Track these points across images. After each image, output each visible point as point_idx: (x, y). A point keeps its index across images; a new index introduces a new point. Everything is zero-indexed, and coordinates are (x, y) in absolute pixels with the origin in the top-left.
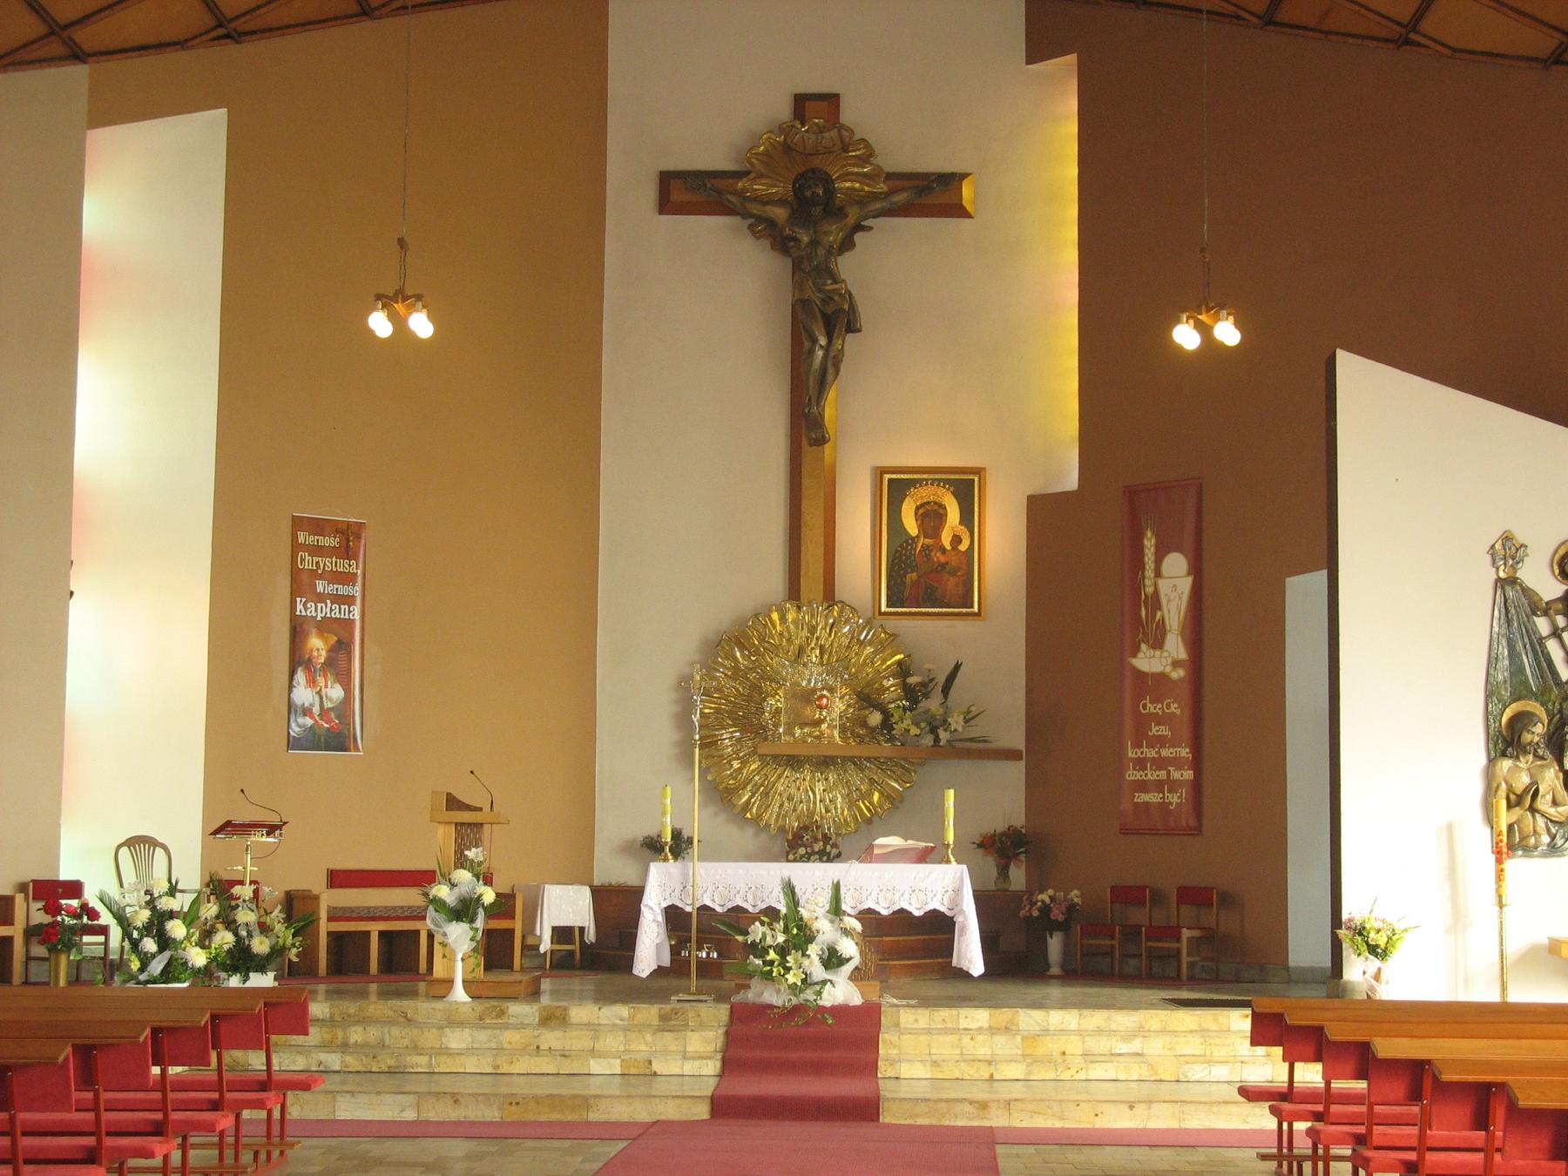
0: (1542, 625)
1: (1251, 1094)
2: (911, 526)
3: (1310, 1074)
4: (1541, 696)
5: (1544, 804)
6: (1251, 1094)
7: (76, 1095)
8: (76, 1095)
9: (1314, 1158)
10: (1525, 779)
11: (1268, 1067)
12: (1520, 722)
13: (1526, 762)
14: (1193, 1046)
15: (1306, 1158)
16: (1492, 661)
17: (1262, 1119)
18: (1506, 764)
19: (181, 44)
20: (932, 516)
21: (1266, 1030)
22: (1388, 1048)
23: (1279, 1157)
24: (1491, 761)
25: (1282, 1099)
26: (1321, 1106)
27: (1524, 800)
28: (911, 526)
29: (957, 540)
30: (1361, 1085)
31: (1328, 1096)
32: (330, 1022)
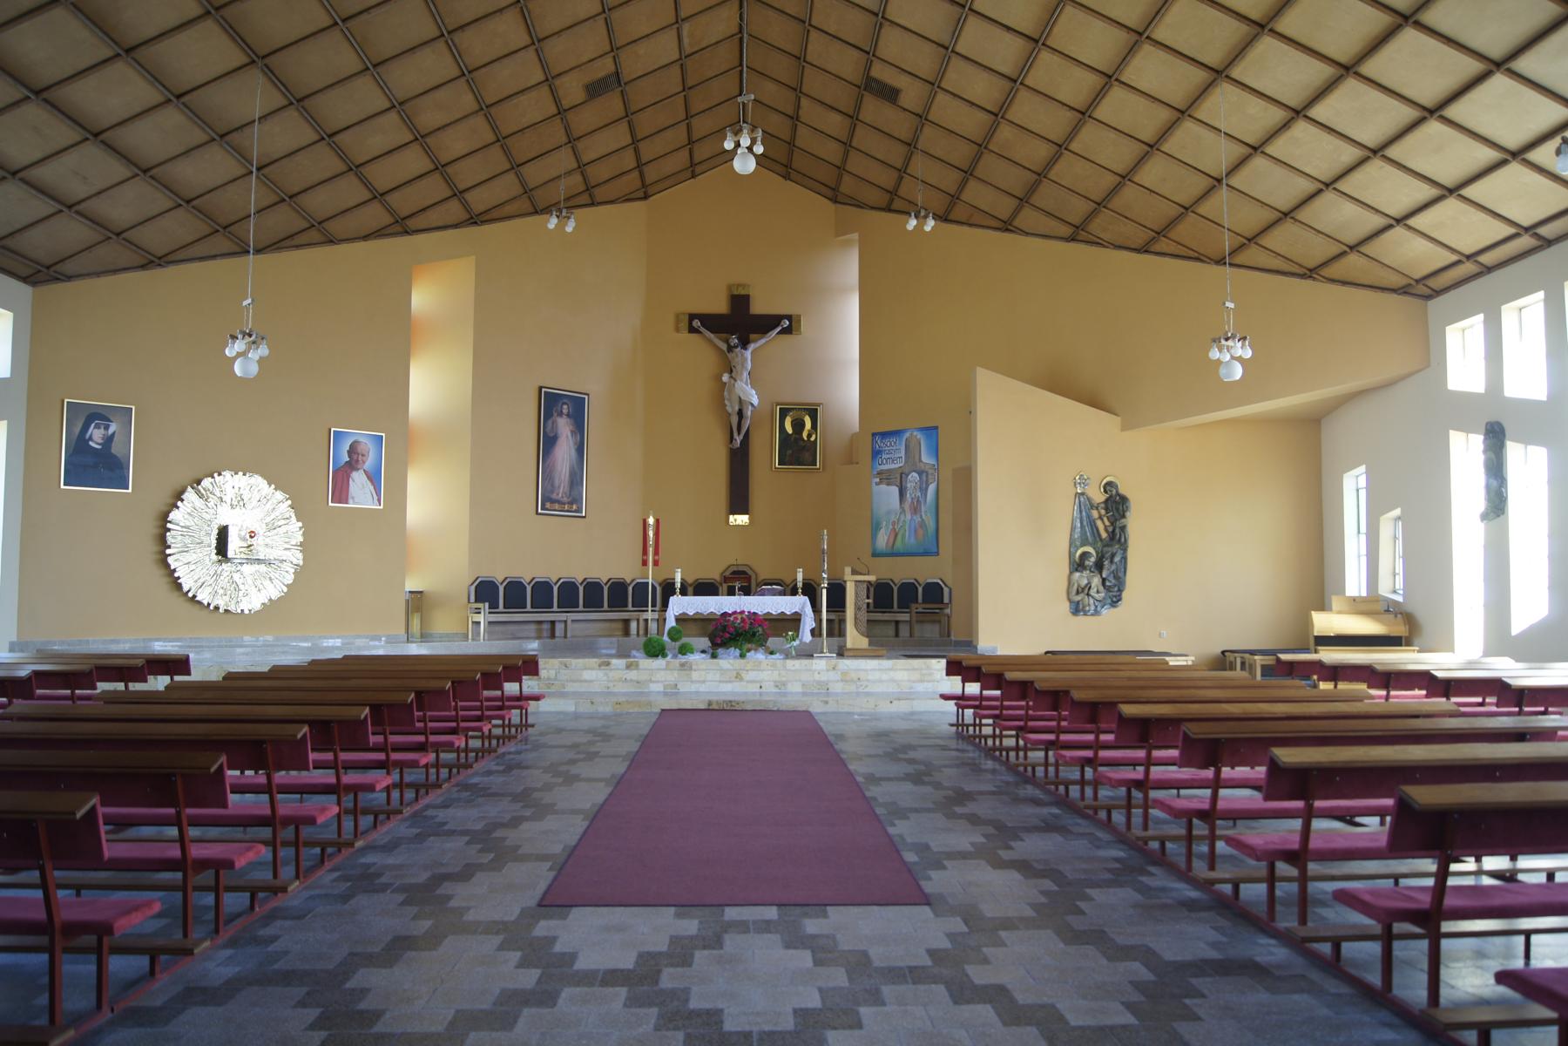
0: (1095, 514)
1: (945, 697)
2: (789, 430)
3: (973, 688)
4: (1093, 545)
5: (1093, 592)
6: (945, 697)
7: (312, 756)
8: (312, 756)
9: (974, 725)
10: (1085, 582)
11: (954, 685)
12: (1085, 555)
13: (1086, 573)
14: (916, 676)
15: (1074, 783)
16: (1073, 529)
17: (951, 706)
18: (1077, 574)
19: (456, 226)
20: (798, 425)
21: (954, 668)
22: (1011, 675)
23: (957, 725)
24: (1071, 573)
25: (961, 700)
26: (978, 703)
27: (1085, 590)
28: (789, 430)
29: (809, 436)
30: (998, 693)
31: (981, 698)
32: (408, 690)
